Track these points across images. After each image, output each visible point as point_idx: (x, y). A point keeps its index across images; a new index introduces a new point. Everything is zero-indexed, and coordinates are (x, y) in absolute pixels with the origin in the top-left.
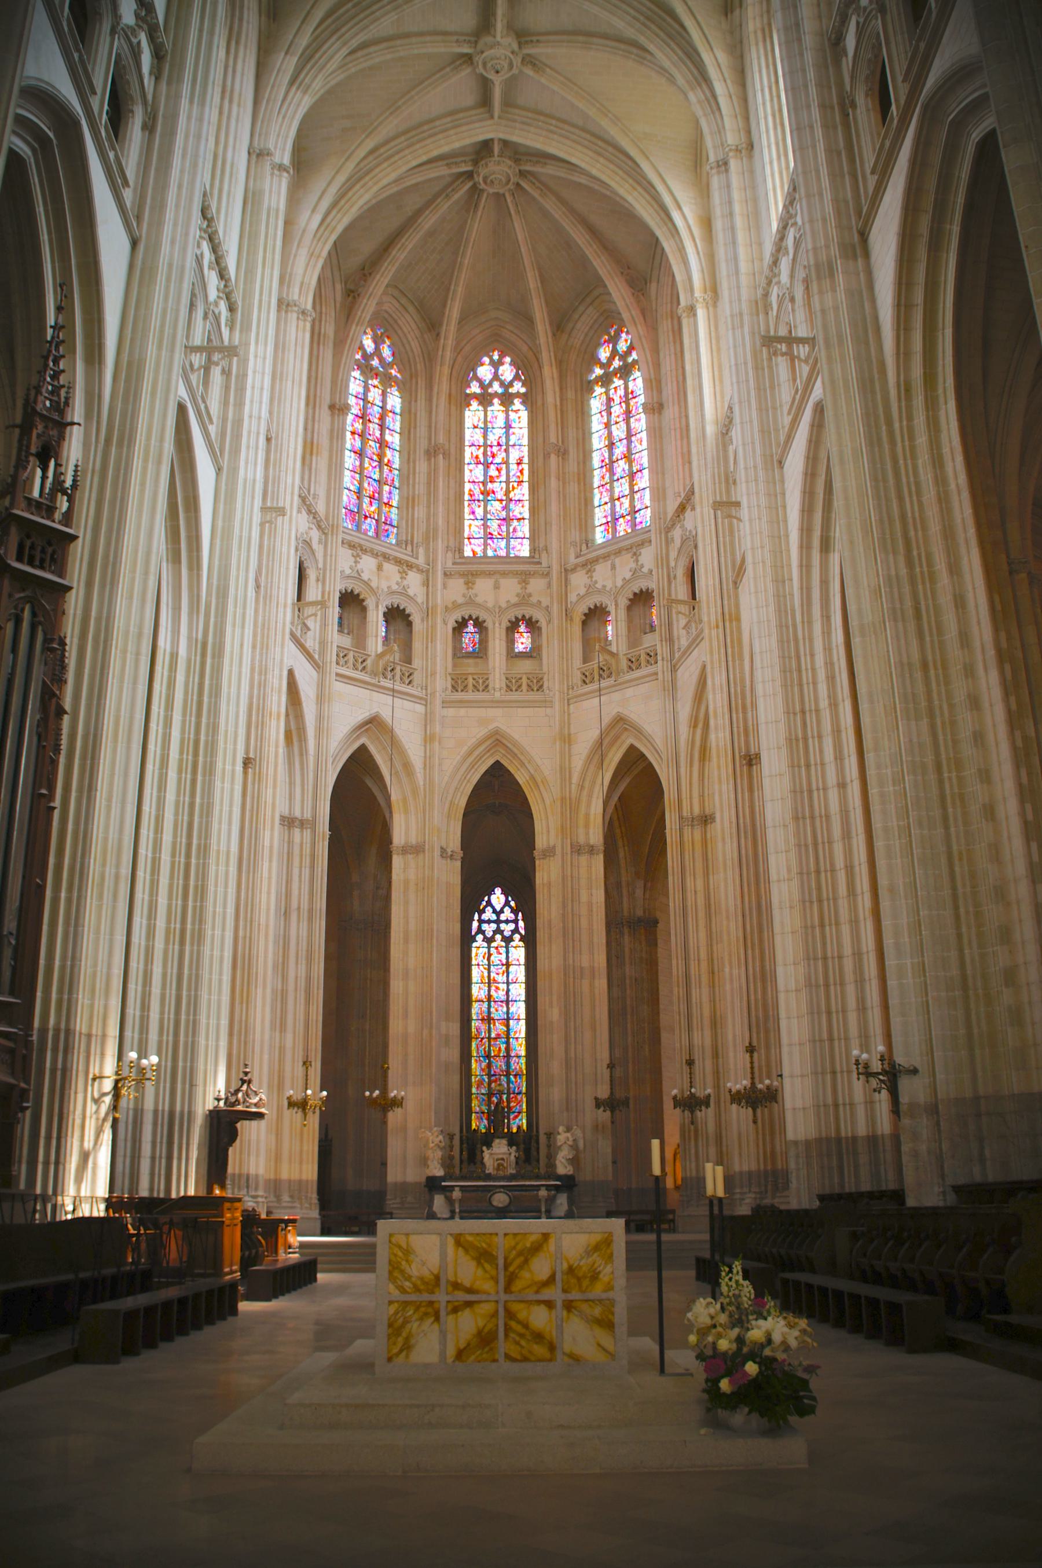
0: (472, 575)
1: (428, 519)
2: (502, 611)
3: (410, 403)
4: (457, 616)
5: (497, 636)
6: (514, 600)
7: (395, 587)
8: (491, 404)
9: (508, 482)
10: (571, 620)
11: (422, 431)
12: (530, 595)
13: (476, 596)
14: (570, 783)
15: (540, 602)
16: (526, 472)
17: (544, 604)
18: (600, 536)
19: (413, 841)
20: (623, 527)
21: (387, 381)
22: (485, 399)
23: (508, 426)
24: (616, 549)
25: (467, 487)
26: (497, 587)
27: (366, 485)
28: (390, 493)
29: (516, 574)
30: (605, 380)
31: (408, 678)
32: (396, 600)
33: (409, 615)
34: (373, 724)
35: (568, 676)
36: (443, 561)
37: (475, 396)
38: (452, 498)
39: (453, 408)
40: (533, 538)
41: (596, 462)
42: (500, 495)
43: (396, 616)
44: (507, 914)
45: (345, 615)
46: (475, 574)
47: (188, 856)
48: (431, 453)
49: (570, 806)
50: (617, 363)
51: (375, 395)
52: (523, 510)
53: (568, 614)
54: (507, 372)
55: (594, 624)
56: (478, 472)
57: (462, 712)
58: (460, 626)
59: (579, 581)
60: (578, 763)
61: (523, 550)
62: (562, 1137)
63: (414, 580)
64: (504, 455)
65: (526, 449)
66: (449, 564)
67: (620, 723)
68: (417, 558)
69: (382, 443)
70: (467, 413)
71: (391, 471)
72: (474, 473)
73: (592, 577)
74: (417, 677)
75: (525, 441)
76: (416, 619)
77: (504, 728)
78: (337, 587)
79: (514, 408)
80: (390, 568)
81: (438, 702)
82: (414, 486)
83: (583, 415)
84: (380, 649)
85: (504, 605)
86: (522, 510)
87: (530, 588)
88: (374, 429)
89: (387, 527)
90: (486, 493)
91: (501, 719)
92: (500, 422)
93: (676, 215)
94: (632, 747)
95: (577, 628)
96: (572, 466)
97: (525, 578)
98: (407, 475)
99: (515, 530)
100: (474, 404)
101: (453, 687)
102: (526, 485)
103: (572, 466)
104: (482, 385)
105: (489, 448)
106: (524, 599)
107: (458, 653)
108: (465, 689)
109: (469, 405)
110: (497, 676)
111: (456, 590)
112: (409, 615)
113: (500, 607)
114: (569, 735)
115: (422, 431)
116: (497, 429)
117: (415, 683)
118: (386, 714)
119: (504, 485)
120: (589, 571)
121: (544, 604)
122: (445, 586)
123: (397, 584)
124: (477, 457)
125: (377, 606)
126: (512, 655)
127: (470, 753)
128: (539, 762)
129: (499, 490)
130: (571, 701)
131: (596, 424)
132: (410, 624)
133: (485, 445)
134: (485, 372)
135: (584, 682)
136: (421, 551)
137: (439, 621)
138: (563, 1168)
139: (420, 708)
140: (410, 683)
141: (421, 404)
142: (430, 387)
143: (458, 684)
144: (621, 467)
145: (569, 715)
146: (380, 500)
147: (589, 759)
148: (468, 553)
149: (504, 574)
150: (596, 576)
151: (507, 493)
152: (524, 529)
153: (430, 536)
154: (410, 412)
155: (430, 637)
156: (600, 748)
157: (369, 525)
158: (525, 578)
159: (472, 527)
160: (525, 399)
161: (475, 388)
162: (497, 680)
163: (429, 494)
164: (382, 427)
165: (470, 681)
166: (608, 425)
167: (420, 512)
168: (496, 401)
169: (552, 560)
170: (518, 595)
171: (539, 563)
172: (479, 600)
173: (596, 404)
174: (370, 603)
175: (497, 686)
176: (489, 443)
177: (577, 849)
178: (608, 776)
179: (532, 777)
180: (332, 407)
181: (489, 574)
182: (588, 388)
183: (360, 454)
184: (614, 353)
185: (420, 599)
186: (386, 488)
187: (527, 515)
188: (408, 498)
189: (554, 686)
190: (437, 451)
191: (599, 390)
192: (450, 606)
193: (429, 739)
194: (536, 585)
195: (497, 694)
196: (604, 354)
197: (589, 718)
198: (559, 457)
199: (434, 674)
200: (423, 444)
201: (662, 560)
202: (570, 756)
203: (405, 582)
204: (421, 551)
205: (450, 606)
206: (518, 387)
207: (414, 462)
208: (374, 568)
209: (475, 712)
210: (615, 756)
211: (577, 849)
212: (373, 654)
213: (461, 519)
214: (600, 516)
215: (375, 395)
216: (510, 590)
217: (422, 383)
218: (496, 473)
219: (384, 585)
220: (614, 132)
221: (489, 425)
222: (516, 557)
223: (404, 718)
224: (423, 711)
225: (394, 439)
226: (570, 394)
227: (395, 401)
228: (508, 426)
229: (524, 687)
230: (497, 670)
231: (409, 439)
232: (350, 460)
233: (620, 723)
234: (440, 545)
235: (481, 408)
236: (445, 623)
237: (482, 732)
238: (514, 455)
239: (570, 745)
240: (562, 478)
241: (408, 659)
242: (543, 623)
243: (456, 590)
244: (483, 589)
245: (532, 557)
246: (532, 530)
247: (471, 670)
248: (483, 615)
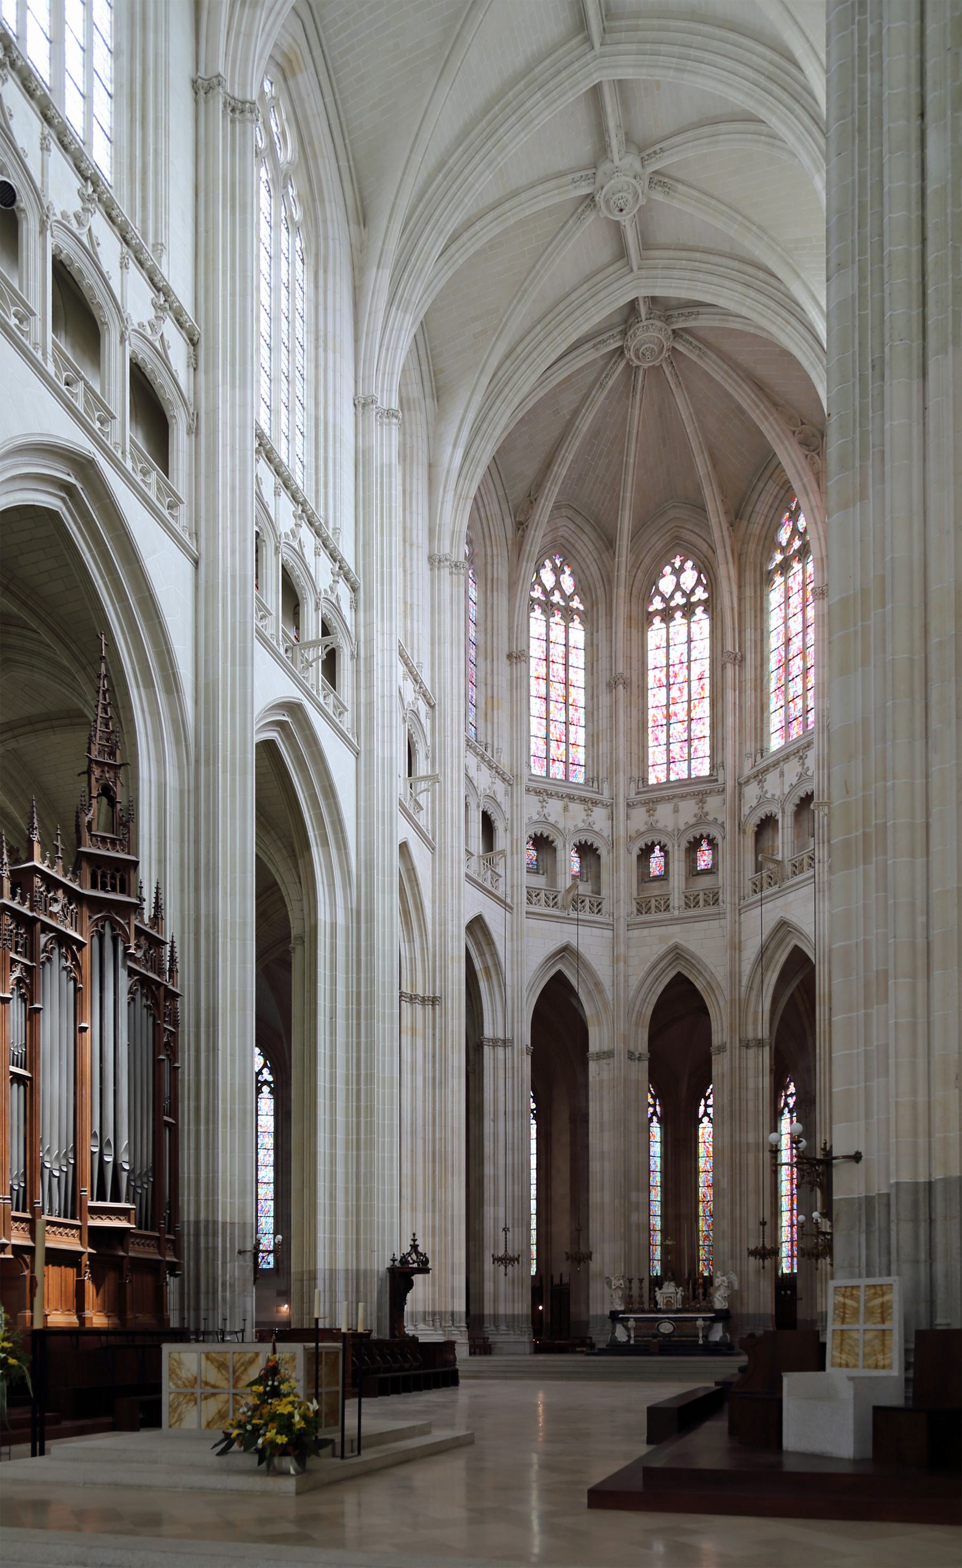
0: (653, 802)
1: (611, 754)
2: (680, 833)
3: (592, 634)
4: (640, 843)
5: (676, 858)
6: (692, 821)
7: (581, 825)
8: (672, 618)
9: (689, 701)
10: (744, 832)
11: (603, 663)
12: (707, 814)
13: (657, 822)
14: (740, 986)
15: (716, 819)
16: (707, 688)
17: (720, 822)
20: (796, 731)
22: (667, 615)
23: (690, 641)
24: (785, 756)
25: (651, 712)
26: (676, 811)
27: (552, 729)
28: (576, 733)
29: (694, 794)
31: (597, 907)
32: (583, 837)
33: (597, 849)
35: (739, 888)
36: (625, 789)
37: (657, 612)
38: (634, 726)
39: (634, 631)
41: (773, 665)
42: (683, 716)
43: (586, 851)
45: (540, 858)
46: (656, 801)
47: (358, 1083)
49: (739, 1007)
52: (702, 729)
55: (768, 834)
57: (646, 932)
60: (747, 968)
61: (703, 769)
63: (599, 814)
64: (686, 672)
65: (707, 662)
66: (633, 794)
68: (602, 794)
69: (567, 684)
70: (650, 634)
71: (576, 710)
72: (656, 697)
73: (762, 787)
74: (605, 907)
75: (707, 653)
76: (603, 852)
77: (682, 942)
78: (524, 834)
79: (694, 618)
81: (622, 926)
82: (598, 721)
84: (568, 885)
85: (682, 827)
86: (702, 727)
87: (707, 807)
88: (558, 670)
89: (575, 767)
90: (668, 717)
91: (678, 935)
94: (796, 947)
96: (749, 673)
97: (701, 797)
98: (591, 713)
99: (695, 749)
100: (657, 620)
101: (638, 910)
102: (707, 701)
104: (664, 599)
105: (671, 669)
106: (701, 819)
107: (644, 877)
108: (648, 911)
109: (651, 623)
110: (676, 896)
111: (639, 817)
112: (597, 849)
113: (679, 829)
114: (740, 942)
115: (603, 663)
117: (603, 911)
119: (686, 705)
120: (760, 781)
121: (720, 822)
122: (628, 817)
123: (583, 821)
124: (660, 680)
125: (565, 846)
126: (693, 872)
127: (653, 968)
128: (713, 970)
129: (680, 711)
130: (742, 911)
132: (599, 857)
133: (668, 666)
134: (666, 584)
135: (755, 891)
136: (606, 786)
137: (622, 851)
139: (608, 933)
140: (599, 911)
143: (643, 907)
145: (740, 924)
146: (567, 742)
149: (683, 797)
150: (767, 786)
151: (689, 711)
153: (613, 769)
154: (592, 643)
155: (615, 868)
157: (557, 771)
158: (701, 797)
161: (657, 604)
162: (676, 900)
163: (611, 729)
164: (566, 666)
165: (653, 902)
167: (604, 747)
168: (678, 615)
170: (695, 816)
171: (716, 780)
172: (660, 825)
175: (676, 905)
176: (671, 663)
178: (772, 977)
179: (709, 983)
181: (669, 799)
185: (606, 833)
186: (572, 728)
187: (707, 732)
188: (593, 736)
189: (726, 897)
190: (618, 685)
192: (634, 835)
193: (615, 960)
194: (713, 803)
195: (676, 913)
197: (756, 925)
199: (618, 901)
202: (740, 962)
203: (591, 819)
204: (606, 786)
205: (634, 835)
207: (598, 697)
208: (560, 809)
209: (656, 931)
212: (563, 890)
216: (689, 810)
218: (679, 693)
219: (570, 825)
221: (671, 643)
222: (697, 777)
223: (592, 943)
224: (611, 936)
225: (578, 677)
228: (690, 641)
229: (701, 903)
230: (676, 890)
231: (592, 674)
234: (622, 778)
235: (664, 625)
236: (629, 851)
237: (663, 948)
238: (696, 669)
239: (740, 951)
241: (598, 892)
242: (719, 840)
243: (639, 817)
244: (664, 813)
245: (711, 775)
246: (712, 748)
247: (656, 892)
248: (664, 840)
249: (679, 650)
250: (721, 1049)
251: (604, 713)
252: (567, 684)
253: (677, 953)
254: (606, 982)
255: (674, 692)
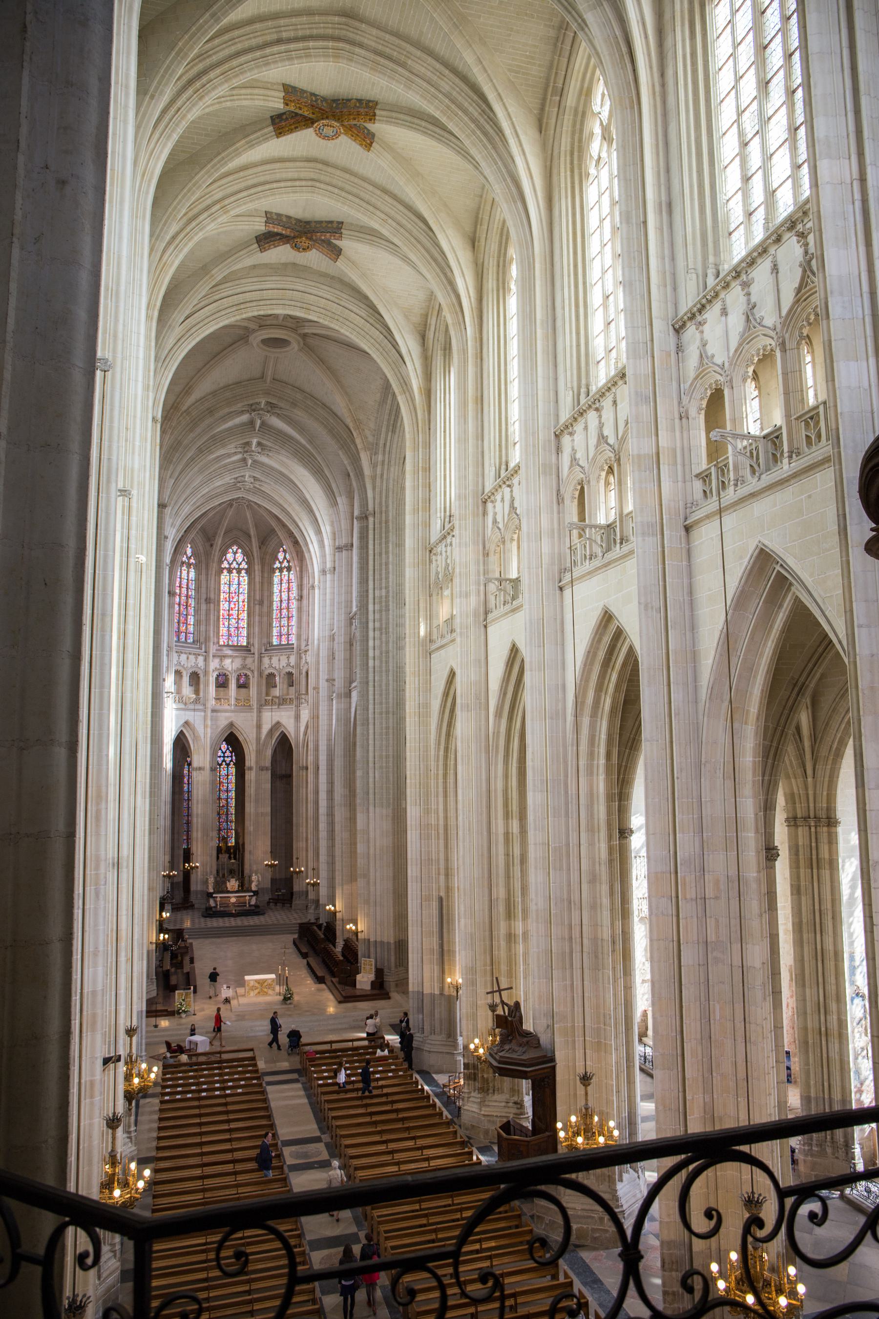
11: (203, 590)
18: (275, 642)
19: (201, 765)
21: (189, 565)
22: (230, 571)
23: (239, 584)
30: (281, 570)
34: (187, 723)
40: (248, 637)
44: (228, 754)
48: (208, 601)
50: (285, 564)
51: (184, 574)
52: (244, 624)
53: (261, 674)
54: (240, 557)
56: (226, 605)
58: (218, 676)
59: (266, 661)
60: (263, 736)
62: (254, 877)
63: (201, 659)
67: (278, 723)
72: (224, 606)
76: (201, 676)
80: (192, 657)
83: (271, 583)
88: (184, 590)
92: (236, 581)
93: (310, 546)
95: (264, 682)
98: (197, 611)
100: (225, 572)
103: (265, 609)
106: (244, 667)
115: (203, 590)
116: (234, 586)
118: (191, 720)
131: (276, 589)
134: (230, 556)
138: (254, 888)
141: (203, 577)
142: (207, 569)
144: (284, 612)
147: (267, 735)
148: (221, 643)
152: (244, 633)
153: (207, 640)
155: (207, 685)
156: (271, 732)
159: (223, 630)
160: (248, 571)
161: (225, 565)
166: (280, 591)
167: (203, 628)
169: (255, 649)
173: (276, 580)
174: (184, 674)
177: (262, 769)
180: (169, 593)
182: (273, 571)
183: (179, 604)
184: (285, 558)
191: (277, 573)
194: (249, 661)
196: (281, 556)
198: (260, 602)
200: (204, 596)
201: (298, 665)
206: (244, 565)
210: (277, 734)
211: (262, 769)
213: (218, 627)
214: (275, 632)
215: (184, 574)
216: (238, 663)
217: (204, 566)
220: (292, 477)
225: (192, 593)
226: (266, 575)
227: (192, 574)
228: (239, 584)
232: (176, 606)
233: (278, 724)
238: (241, 598)
240: (261, 615)
244: (227, 662)
246: (248, 634)
249: (234, 586)
250: (250, 769)
251: (203, 612)
252: (187, 596)
253: (231, 725)
254: (202, 736)
255: (232, 606)
